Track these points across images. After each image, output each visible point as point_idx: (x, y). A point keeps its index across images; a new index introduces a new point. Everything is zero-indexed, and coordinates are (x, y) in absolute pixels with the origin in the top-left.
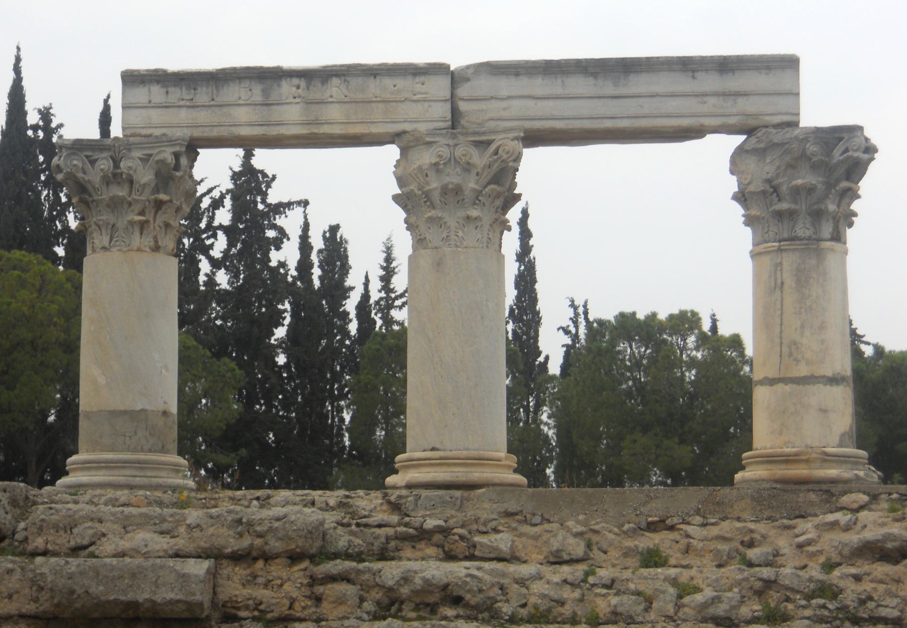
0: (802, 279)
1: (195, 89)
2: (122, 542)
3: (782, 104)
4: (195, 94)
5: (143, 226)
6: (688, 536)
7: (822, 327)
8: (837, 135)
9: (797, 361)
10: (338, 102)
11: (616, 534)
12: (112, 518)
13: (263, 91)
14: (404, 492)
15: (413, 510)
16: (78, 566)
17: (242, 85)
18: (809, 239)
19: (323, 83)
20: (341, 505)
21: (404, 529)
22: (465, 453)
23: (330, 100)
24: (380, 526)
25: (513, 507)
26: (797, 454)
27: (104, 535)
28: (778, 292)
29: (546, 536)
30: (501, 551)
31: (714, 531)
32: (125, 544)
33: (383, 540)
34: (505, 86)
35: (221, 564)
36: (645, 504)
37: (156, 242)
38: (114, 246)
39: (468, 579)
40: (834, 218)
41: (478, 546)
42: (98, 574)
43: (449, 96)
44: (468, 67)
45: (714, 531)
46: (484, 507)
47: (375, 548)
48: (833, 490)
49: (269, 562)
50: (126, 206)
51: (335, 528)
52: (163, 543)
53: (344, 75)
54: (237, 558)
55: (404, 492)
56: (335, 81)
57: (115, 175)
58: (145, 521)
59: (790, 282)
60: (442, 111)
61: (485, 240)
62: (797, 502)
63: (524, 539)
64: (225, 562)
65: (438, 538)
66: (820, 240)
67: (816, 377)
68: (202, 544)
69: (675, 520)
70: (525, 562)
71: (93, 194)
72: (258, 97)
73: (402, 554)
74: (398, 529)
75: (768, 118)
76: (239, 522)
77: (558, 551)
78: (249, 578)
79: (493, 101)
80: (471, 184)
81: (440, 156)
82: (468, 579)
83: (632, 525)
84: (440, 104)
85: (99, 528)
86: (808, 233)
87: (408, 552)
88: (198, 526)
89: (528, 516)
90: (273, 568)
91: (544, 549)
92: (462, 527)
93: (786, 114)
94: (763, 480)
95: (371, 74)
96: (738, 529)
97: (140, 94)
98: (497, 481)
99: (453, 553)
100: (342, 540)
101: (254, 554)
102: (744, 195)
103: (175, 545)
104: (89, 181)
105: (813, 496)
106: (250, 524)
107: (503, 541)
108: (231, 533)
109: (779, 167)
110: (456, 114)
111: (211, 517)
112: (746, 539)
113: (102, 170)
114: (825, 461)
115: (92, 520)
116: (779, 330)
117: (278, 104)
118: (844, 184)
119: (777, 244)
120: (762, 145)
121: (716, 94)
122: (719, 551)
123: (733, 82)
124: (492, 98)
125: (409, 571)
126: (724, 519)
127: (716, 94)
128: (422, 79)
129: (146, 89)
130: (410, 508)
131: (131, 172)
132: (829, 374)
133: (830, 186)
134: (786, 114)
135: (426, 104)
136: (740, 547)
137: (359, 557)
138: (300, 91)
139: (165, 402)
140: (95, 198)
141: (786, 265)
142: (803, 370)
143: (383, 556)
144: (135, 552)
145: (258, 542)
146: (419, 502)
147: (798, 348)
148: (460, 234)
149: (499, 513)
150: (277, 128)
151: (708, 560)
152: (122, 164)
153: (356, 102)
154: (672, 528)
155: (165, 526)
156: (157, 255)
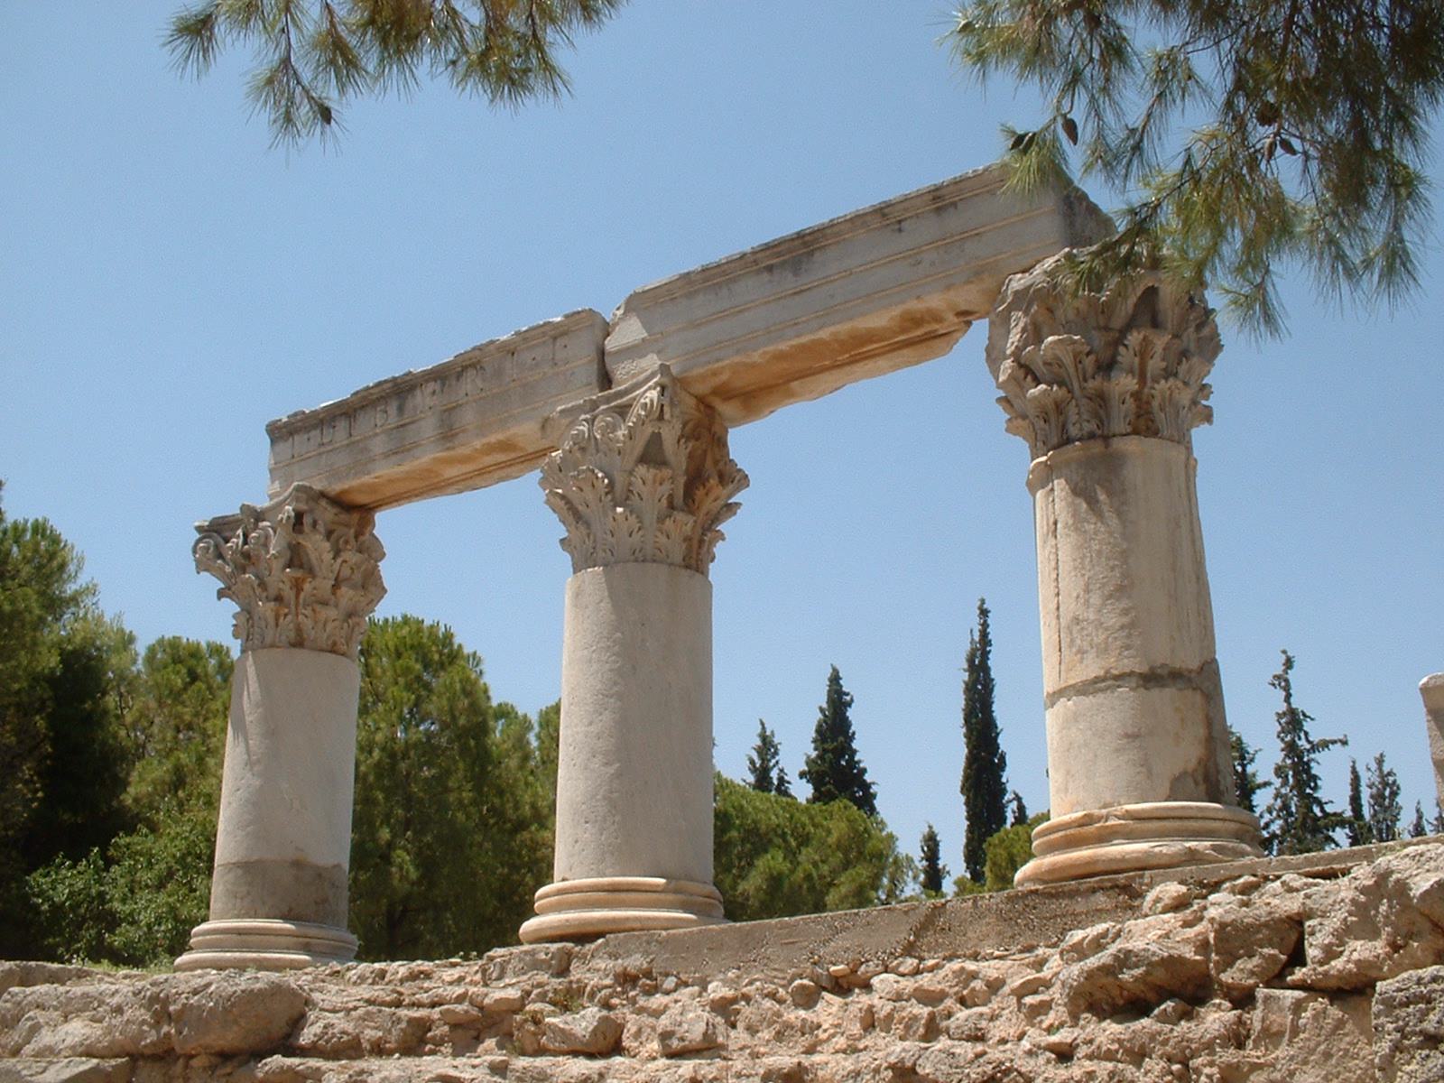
36: (825, 942)
66: (1106, 439)
117: (412, 422)
139: (297, 848)
156: (296, 651)
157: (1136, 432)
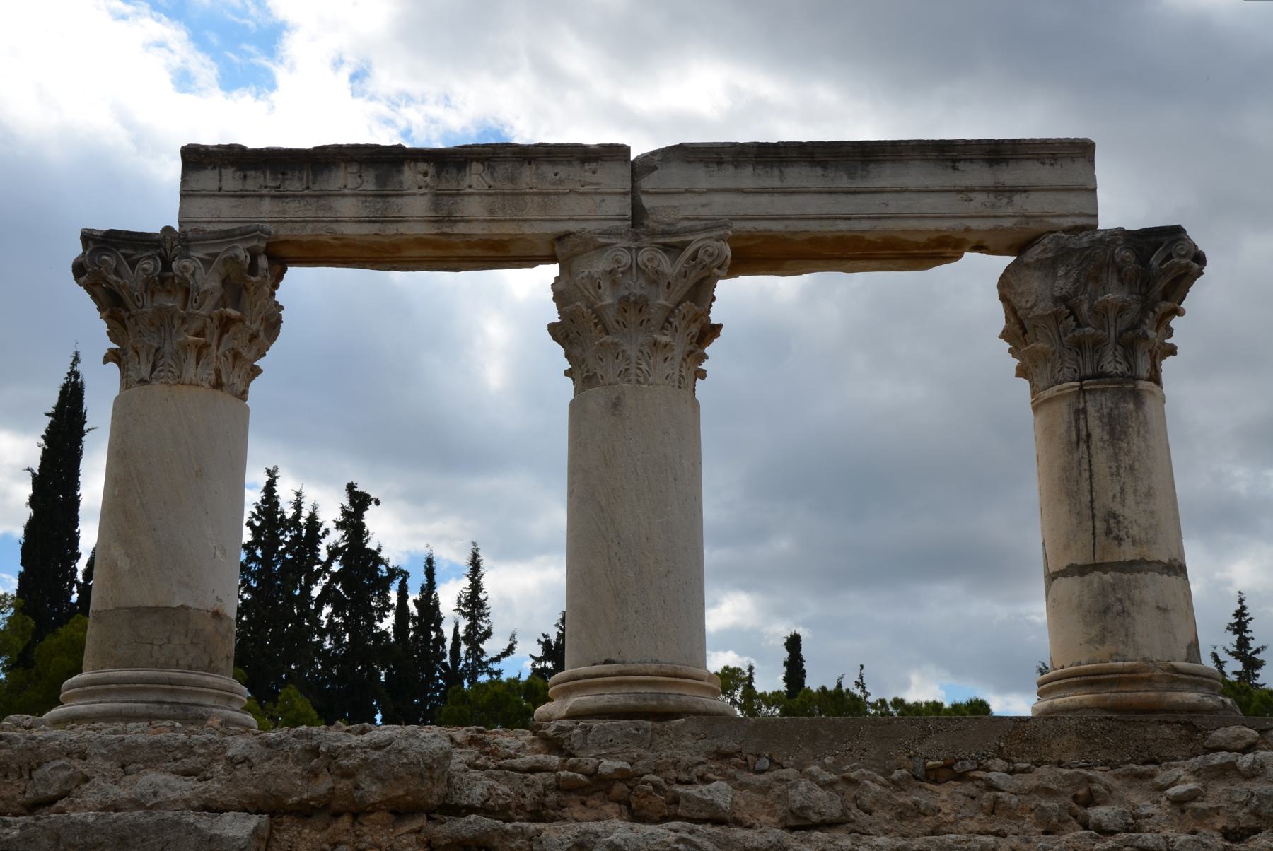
0: (1116, 429)
1: (283, 174)
2: (116, 789)
3: (1075, 202)
4: (283, 181)
5: (201, 350)
6: (991, 787)
7: (1149, 495)
8: (1153, 239)
9: (1119, 540)
10: (479, 194)
11: (884, 785)
12: (103, 751)
13: (377, 177)
14: (566, 723)
15: (581, 748)
16: (26, 826)
17: (349, 170)
18: (1123, 375)
19: (459, 171)
20: (472, 741)
21: (571, 774)
22: (654, 667)
23: (469, 190)
24: (532, 770)
25: (729, 744)
26: (1133, 670)
27: (87, 779)
28: (1083, 446)
29: (779, 788)
30: (718, 807)
31: (1030, 781)
32: (119, 792)
33: (540, 788)
34: (702, 177)
35: (280, 824)
36: (920, 740)
37: (218, 374)
38: (157, 379)
39: (681, 846)
40: (1150, 351)
41: (682, 801)
42: (58, 839)
43: (629, 189)
44: (654, 153)
45: (1030, 781)
46: (686, 747)
47: (527, 801)
48: (1197, 722)
49: (360, 819)
50: (177, 323)
51: (466, 771)
52: (186, 788)
53: (488, 159)
54: (304, 812)
55: (566, 723)
56: (476, 167)
57: (163, 280)
58: (157, 755)
59: (1098, 433)
60: (621, 206)
61: (676, 377)
62: (1145, 740)
63: (746, 792)
64: (287, 820)
65: (619, 788)
66: (1136, 378)
67: (1148, 562)
68: (251, 790)
69: (968, 766)
70: (750, 827)
71: (131, 306)
72: (370, 186)
73: (567, 813)
74: (563, 774)
75: (1055, 221)
76: (315, 752)
77: (803, 808)
78: (326, 846)
79: (688, 195)
80: (661, 300)
81: (618, 261)
82: (681, 846)
83: (904, 771)
84: (617, 198)
85: (80, 768)
86: (1121, 368)
87: (576, 810)
88: (246, 760)
89: (750, 758)
90: (365, 829)
91: (778, 807)
92: (655, 772)
93: (1080, 215)
94: (1087, 708)
95: (525, 159)
96: (1066, 777)
97: (208, 180)
98: (700, 707)
99: (644, 812)
100: (477, 789)
101: (336, 805)
102: (1022, 327)
103: (205, 791)
104: (124, 286)
105: (1166, 731)
106: (332, 755)
107: (719, 793)
108: (299, 770)
109: (1077, 280)
110: (638, 214)
111: (269, 745)
112: (1080, 792)
113: (144, 270)
114: (1175, 680)
115: (68, 755)
116: (1089, 499)
117: (397, 196)
118: (1166, 306)
119: (1078, 384)
120: (1050, 255)
121: (985, 190)
122: (1043, 809)
123: (1010, 175)
124: (687, 191)
125: (585, 833)
126: (1039, 764)
127: (985, 190)
128: (593, 165)
129: (217, 171)
130: (577, 745)
131: (187, 275)
132: (1166, 560)
133: (1147, 306)
134: (1080, 215)
135: (598, 198)
136: (1074, 805)
137: (503, 813)
138: (428, 179)
139: (217, 599)
140: (133, 312)
141: (1091, 410)
142: (1128, 553)
143: (536, 817)
144: (137, 803)
145: (344, 784)
146: (590, 737)
147: (1118, 522)
148: (644, 366)
149: (707, 753)
150: (395, 226)
151: (1029, 822)
152: (174, 265)
153: (504, 194)
154: (962, 777)
155: (190, 763)
156: (218, 393)
157: (1149, 379)
